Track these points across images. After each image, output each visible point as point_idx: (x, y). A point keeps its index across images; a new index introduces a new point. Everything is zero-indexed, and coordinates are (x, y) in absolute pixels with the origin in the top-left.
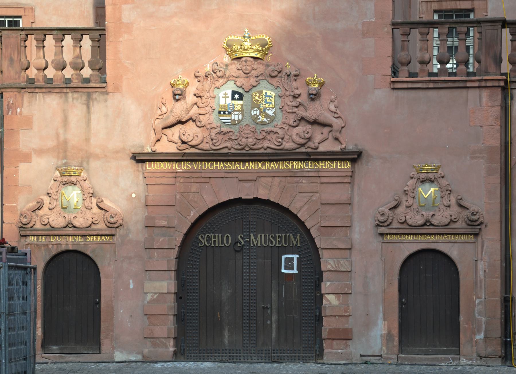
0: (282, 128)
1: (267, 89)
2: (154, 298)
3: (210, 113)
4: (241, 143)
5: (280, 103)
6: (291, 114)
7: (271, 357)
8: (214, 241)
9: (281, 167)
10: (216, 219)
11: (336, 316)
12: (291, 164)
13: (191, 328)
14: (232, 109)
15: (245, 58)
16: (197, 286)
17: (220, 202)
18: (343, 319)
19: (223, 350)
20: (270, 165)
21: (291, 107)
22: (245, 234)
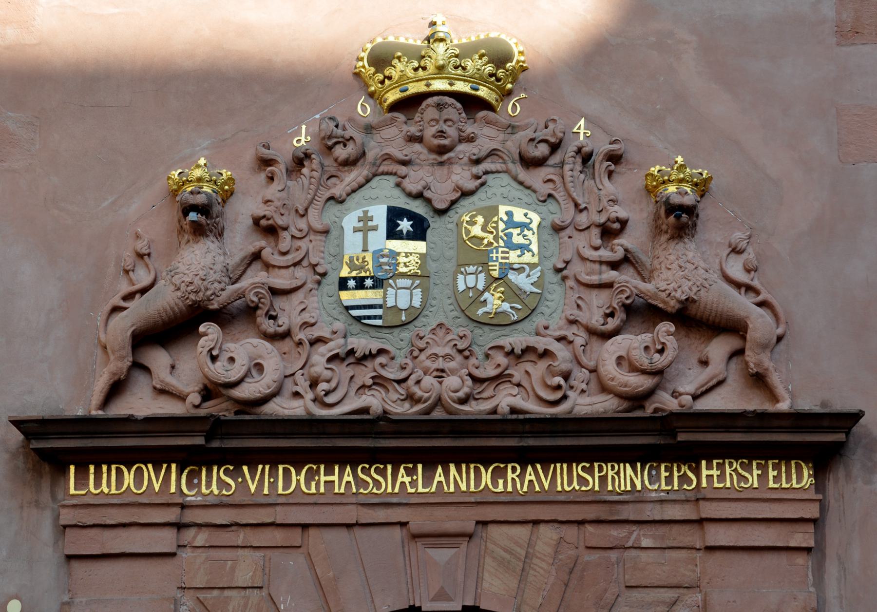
0: (564, 342)
1: (511, 201)
3: (310, 285)
4: (418, 392)
5: (557, 252)
6: (595, 292)
9: (563, 484)
12: (597, 475)
14: (388, 268)
15: (436, 99)
20: (522, 476)
21: (597, 266)
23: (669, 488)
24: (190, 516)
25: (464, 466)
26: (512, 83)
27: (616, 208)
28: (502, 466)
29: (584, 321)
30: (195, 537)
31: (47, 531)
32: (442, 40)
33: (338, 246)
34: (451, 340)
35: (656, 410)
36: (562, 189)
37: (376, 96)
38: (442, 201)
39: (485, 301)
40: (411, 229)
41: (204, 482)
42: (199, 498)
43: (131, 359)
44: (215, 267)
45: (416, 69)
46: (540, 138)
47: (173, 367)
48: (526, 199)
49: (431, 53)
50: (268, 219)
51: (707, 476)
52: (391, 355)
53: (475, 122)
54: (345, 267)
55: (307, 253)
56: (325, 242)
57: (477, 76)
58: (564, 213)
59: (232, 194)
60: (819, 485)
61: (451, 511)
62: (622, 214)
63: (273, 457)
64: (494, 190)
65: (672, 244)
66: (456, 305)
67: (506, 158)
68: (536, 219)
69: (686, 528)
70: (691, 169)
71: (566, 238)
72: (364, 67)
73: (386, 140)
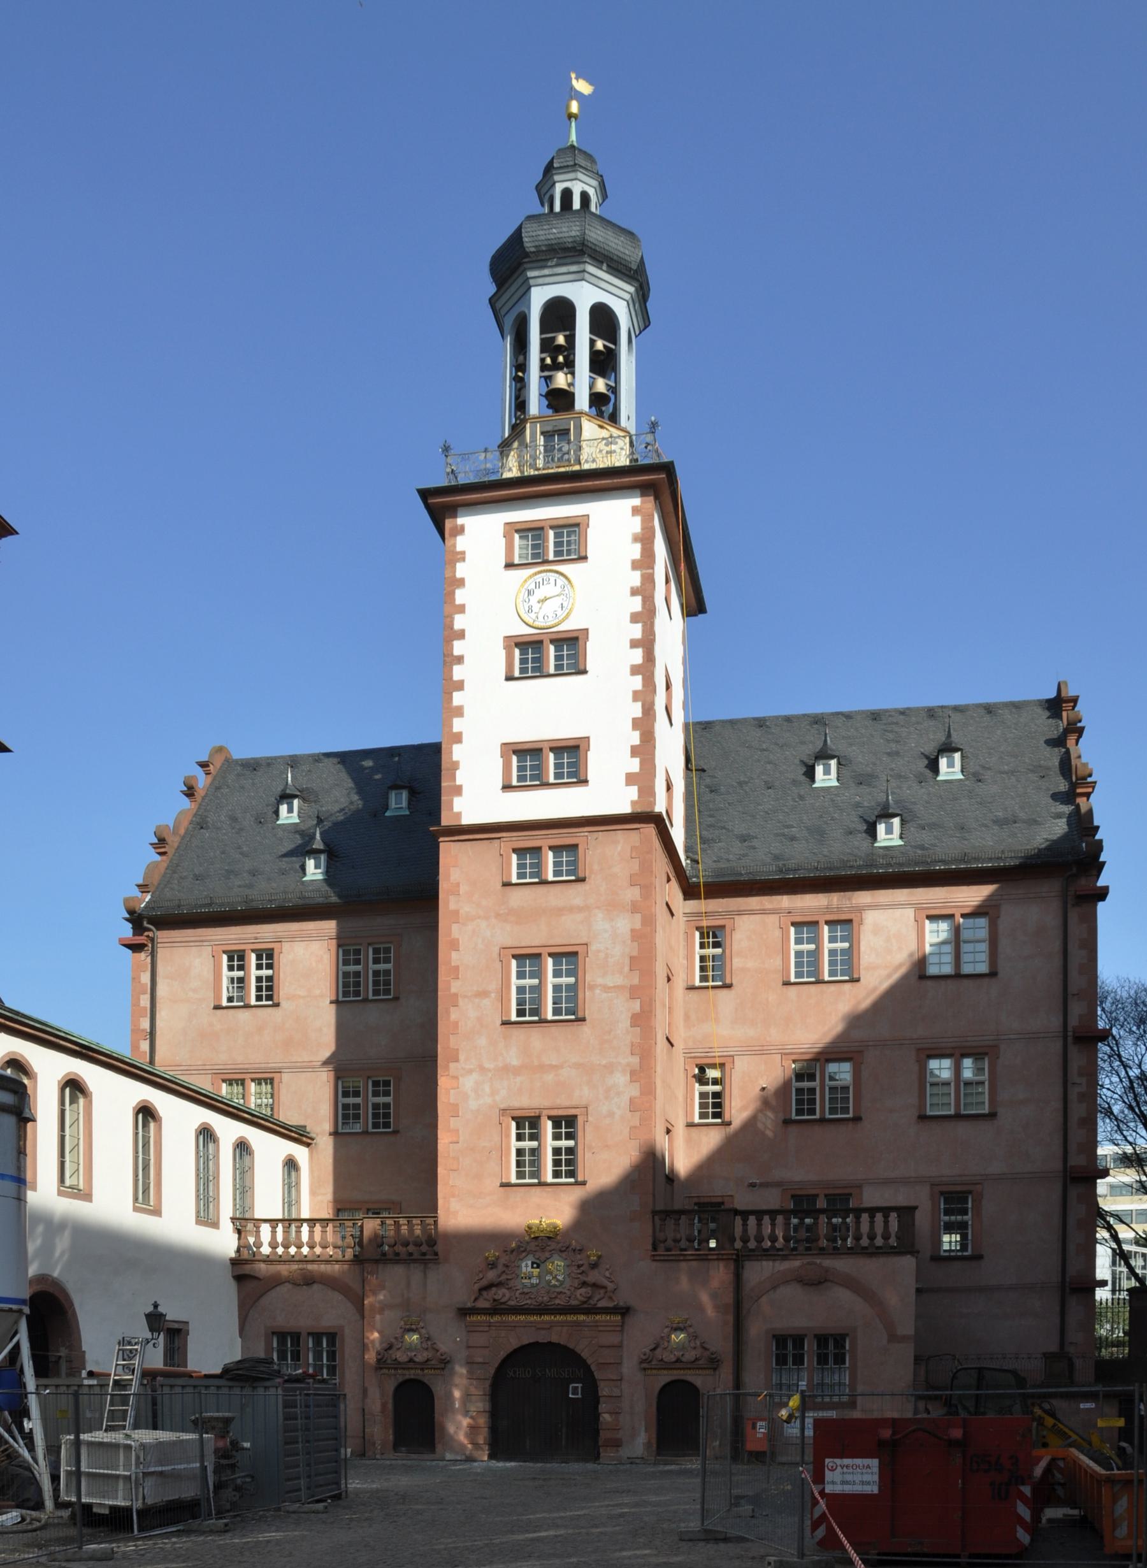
9: (568, 1318)
68: (563, 1264)
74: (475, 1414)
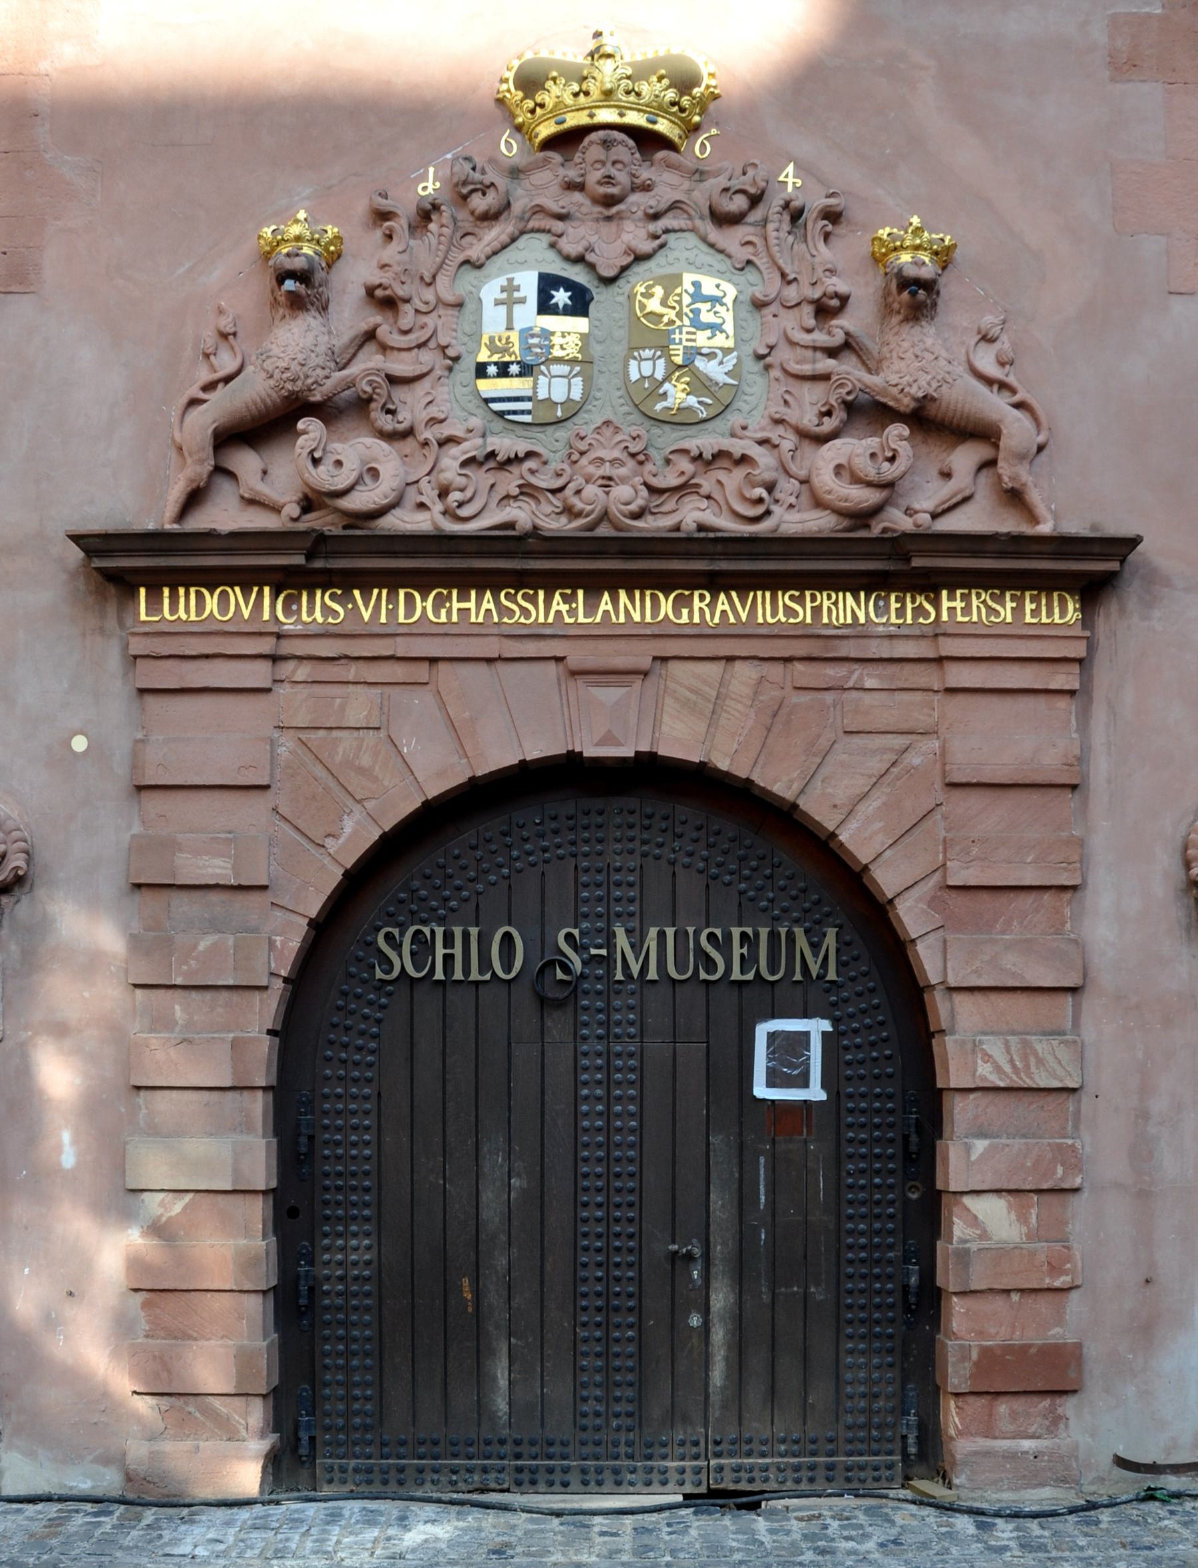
0: (766, 445)
1: (699, 269)
2: (173, 1213)
3: (438, 372)
4: (579, 505)
5: (758, 334)
6: (807, 386)
7: (705, 1471)
8: (449, 959)
10: (457, 857)
11: (1007, 1292)
12: (809, 605)
13: (341, 1347)
14: (538, 350)
15: (601, 134)
16: (368, 1159)
17: (479, 773)
18: (1043, 1304)
19: (488, 1443)
20: (712, 605)
21: (809, 353)
22: (585, 925)
23: (901, 621)
24: (287, 647)
25: (637, 594)
26: (700, 114)
27: (834, 280)
28: (687, 593)
29: (793, 421)
30: (294, 672)
31: (114, 661)
32: (609, 56)
33: (475, 322)
34: (620, 442)
35: (885, 530)
36: (764, 254)
37: (525, 129)
38: (609, 267)
39: (665, 393)
40: (569, 302)
41: (304, 609)
42: (299, 627)
43: (213, 463)
44: (317, 349)
45: (576, 95)
46: (737, 188)
47: (265, 472)
48: (718, 266)
49: (596, 73)
50: (385, 289)
51: (949, 608)
52: (544, 459)
53: (652, 165)
54: (484, 349)
55: (435, 332)
56: (458, 318)
57: (654, 104)
58: (768, 286)
59: (339, 257)
60: (1087, 620)
61: (622, 645)
62: (842, 287)
63: (393, 580)
64: (676, 254)
65: (906, 328)
66: (627, 398)
67: (693, 213)
68: (730, 292)
69: (921, 667)
70: (930, 234)
71: (770, 317)
72: (509, 91)
73: (537, 187)
74: (178, 1206)
